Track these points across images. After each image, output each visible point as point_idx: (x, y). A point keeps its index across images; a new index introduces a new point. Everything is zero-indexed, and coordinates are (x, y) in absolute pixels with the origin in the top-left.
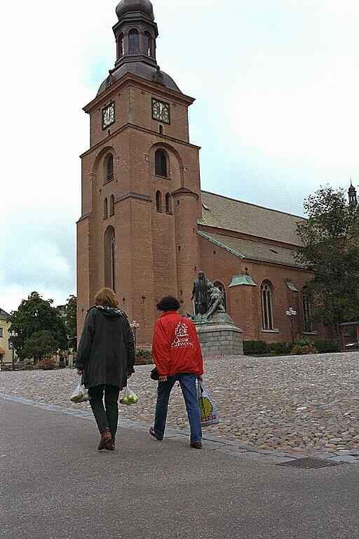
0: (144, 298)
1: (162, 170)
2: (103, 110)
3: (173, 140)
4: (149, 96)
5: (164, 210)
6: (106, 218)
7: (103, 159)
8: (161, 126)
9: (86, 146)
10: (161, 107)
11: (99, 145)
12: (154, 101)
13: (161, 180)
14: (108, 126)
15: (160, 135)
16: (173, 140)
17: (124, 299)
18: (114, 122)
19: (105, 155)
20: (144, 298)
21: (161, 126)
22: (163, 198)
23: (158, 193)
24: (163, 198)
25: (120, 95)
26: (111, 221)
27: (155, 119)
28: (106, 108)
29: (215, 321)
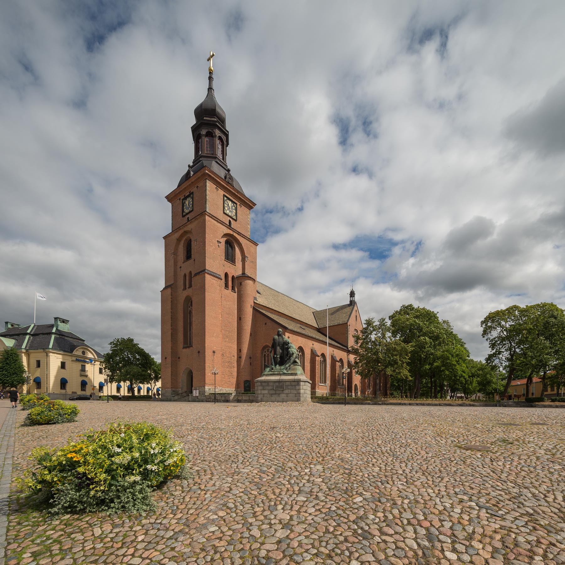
0: (214, 352)
1: (230, 257)
2: (183, 200)
3: (239, 234)
4: (221, 192)
5: (230, 288)
6: (185, 289)
7: (182, 243)
8: (230, 221)
9: (168, 230)
10: (230, 203)
11: (179, 228)
12: (225, 198)
13: (228, 265)
14: (187, 214)
15: (229, 226)
16: (239, 234)
17: (199, 352)
18: (192, 211)
19: (184, 239)
20: (214, 352)
21: (230, 221)
22: (230, 279)
23: (226, 275)
24: (230, 279)
25: (197, 187)
26: (189, 292)
27: (224, 213)
28: (185, 198)
29: (292, 372)
